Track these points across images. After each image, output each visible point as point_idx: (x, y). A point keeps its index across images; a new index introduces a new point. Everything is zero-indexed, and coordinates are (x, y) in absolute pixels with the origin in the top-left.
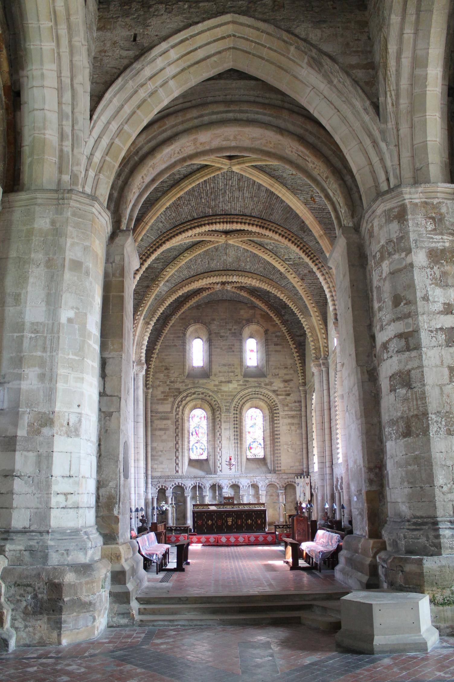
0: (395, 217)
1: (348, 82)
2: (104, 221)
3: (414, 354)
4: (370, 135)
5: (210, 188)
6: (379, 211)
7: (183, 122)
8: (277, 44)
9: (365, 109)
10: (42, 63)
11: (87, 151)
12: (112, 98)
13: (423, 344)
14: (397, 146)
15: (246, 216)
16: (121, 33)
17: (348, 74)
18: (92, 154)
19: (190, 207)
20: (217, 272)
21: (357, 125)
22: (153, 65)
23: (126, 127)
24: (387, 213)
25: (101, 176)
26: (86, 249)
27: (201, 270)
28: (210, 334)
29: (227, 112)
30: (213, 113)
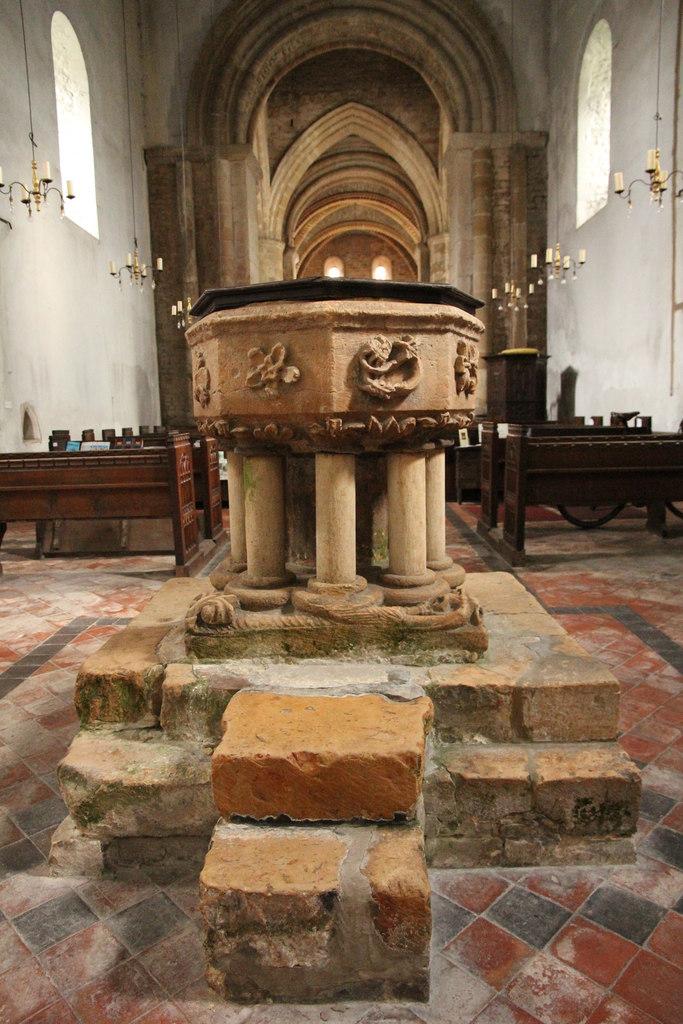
1: (422, 153)
2: (281, 247)
4: (434, 189)
8: (380, 123)
12: (281, 169)
16: (283, 120)
17: (422, 147)
18: (272, 206)
21: (427, 181)
24: (436, 246)
26: (276, 270)
28: (345, 266)
29: (351, 160)
30: (341, 162)
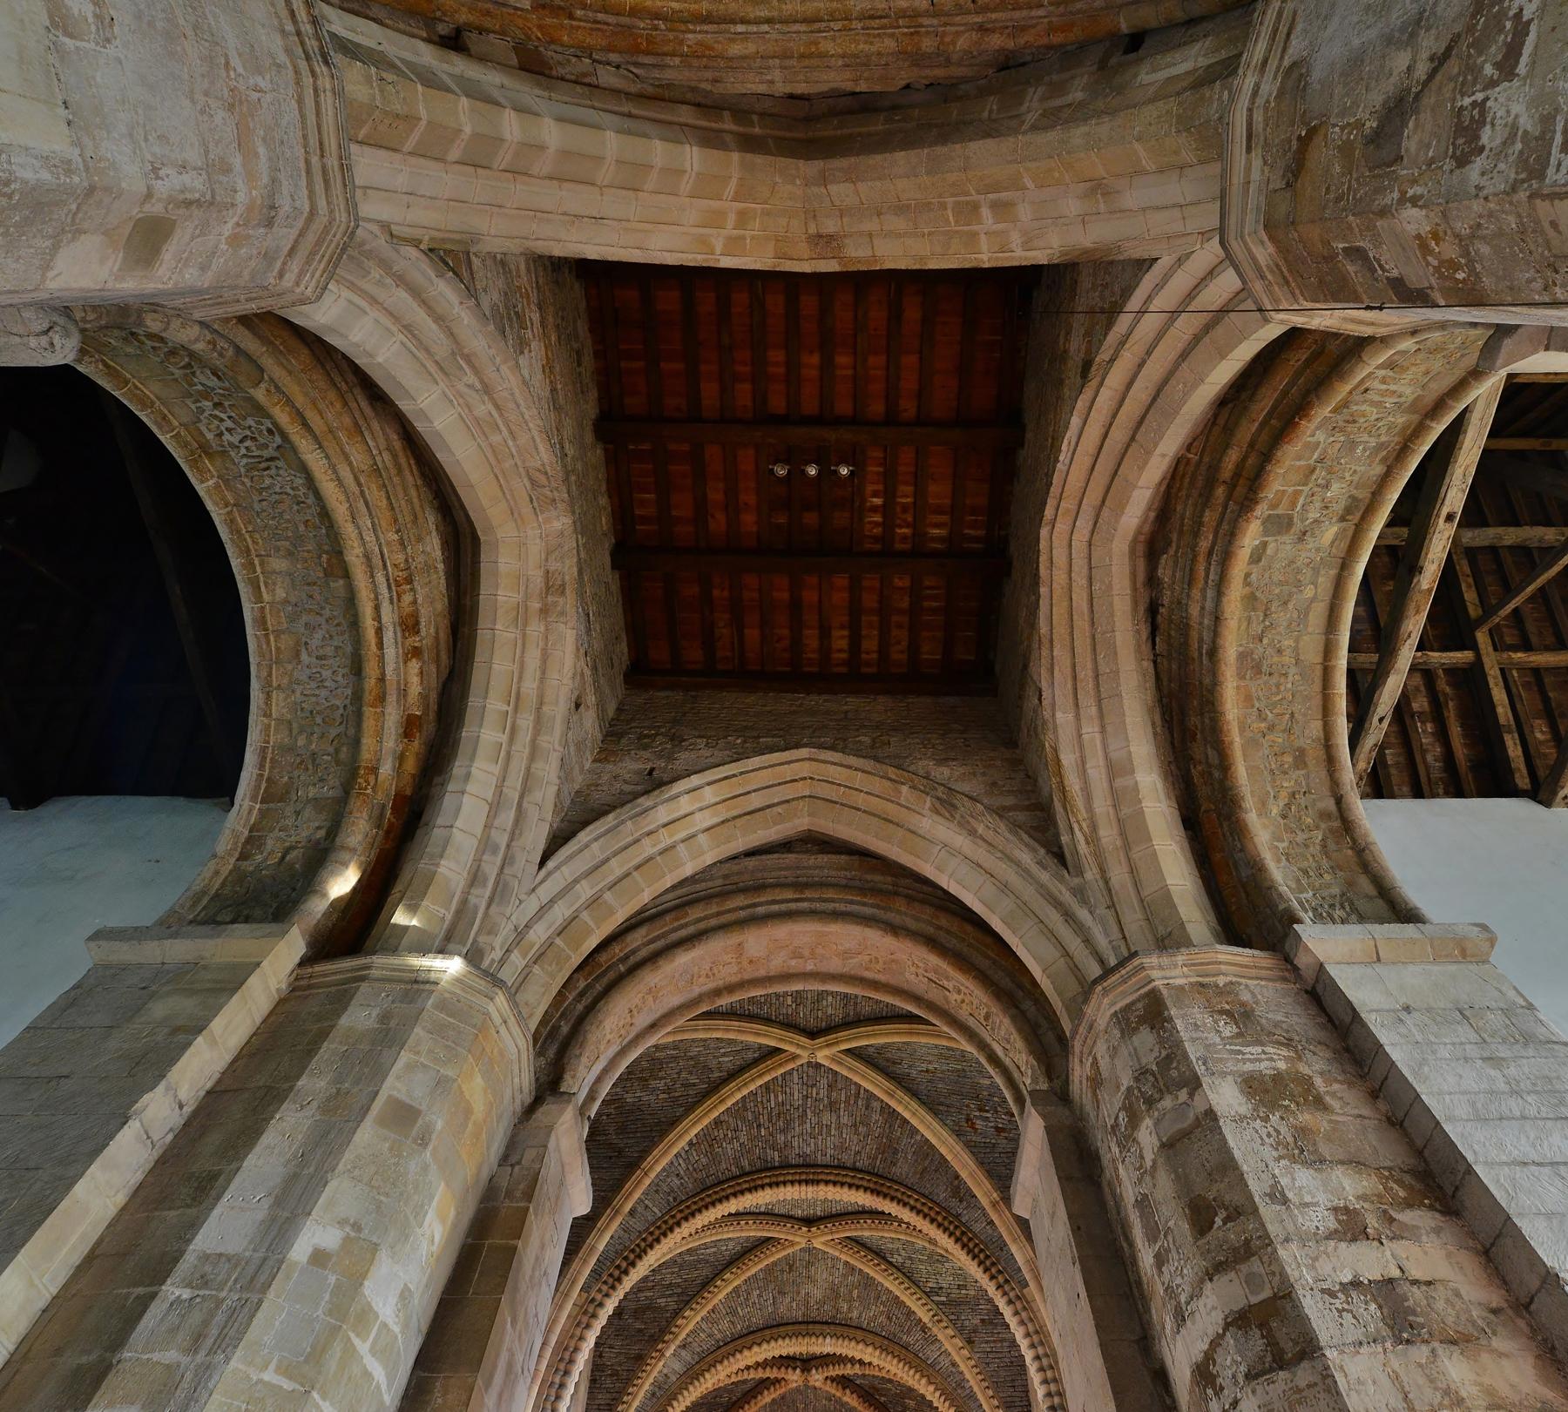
0: (1142, 1020)
3: (1304, 1374)
4: (1057, 904)
5: (777, 1104)
6: (1102, 1022)
7: (718, 914)
8: (877, 785)
9: (1039, 863)
10: (472, 759)
11: (521, 916)
12: (590, 843)
13: (1323, 1338)
14: (1112, 906)
15: (845, 1168)
17: (1001, 817)
19: (736, 1145)
20: (790, 1327)
21: (1028, 892)
22: (672, 805)
23: (608, 896)
25: (536, 969)
27: (757, 1320)
29: (797, 900)
